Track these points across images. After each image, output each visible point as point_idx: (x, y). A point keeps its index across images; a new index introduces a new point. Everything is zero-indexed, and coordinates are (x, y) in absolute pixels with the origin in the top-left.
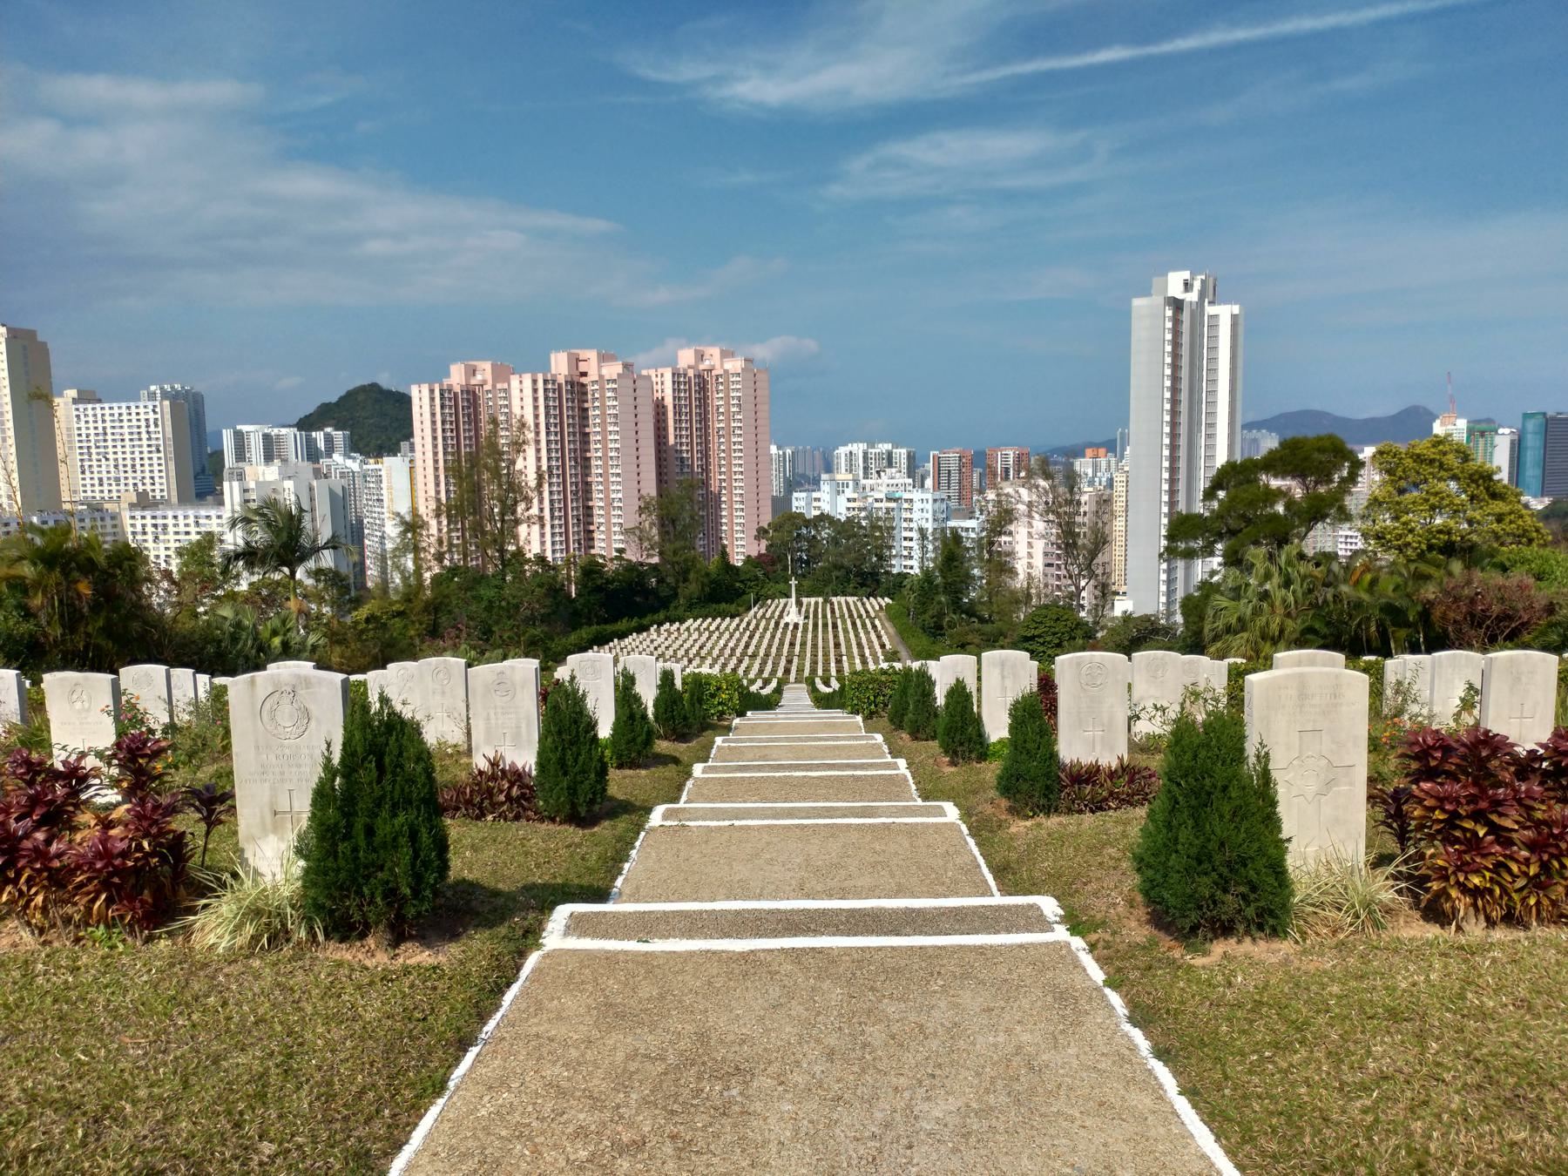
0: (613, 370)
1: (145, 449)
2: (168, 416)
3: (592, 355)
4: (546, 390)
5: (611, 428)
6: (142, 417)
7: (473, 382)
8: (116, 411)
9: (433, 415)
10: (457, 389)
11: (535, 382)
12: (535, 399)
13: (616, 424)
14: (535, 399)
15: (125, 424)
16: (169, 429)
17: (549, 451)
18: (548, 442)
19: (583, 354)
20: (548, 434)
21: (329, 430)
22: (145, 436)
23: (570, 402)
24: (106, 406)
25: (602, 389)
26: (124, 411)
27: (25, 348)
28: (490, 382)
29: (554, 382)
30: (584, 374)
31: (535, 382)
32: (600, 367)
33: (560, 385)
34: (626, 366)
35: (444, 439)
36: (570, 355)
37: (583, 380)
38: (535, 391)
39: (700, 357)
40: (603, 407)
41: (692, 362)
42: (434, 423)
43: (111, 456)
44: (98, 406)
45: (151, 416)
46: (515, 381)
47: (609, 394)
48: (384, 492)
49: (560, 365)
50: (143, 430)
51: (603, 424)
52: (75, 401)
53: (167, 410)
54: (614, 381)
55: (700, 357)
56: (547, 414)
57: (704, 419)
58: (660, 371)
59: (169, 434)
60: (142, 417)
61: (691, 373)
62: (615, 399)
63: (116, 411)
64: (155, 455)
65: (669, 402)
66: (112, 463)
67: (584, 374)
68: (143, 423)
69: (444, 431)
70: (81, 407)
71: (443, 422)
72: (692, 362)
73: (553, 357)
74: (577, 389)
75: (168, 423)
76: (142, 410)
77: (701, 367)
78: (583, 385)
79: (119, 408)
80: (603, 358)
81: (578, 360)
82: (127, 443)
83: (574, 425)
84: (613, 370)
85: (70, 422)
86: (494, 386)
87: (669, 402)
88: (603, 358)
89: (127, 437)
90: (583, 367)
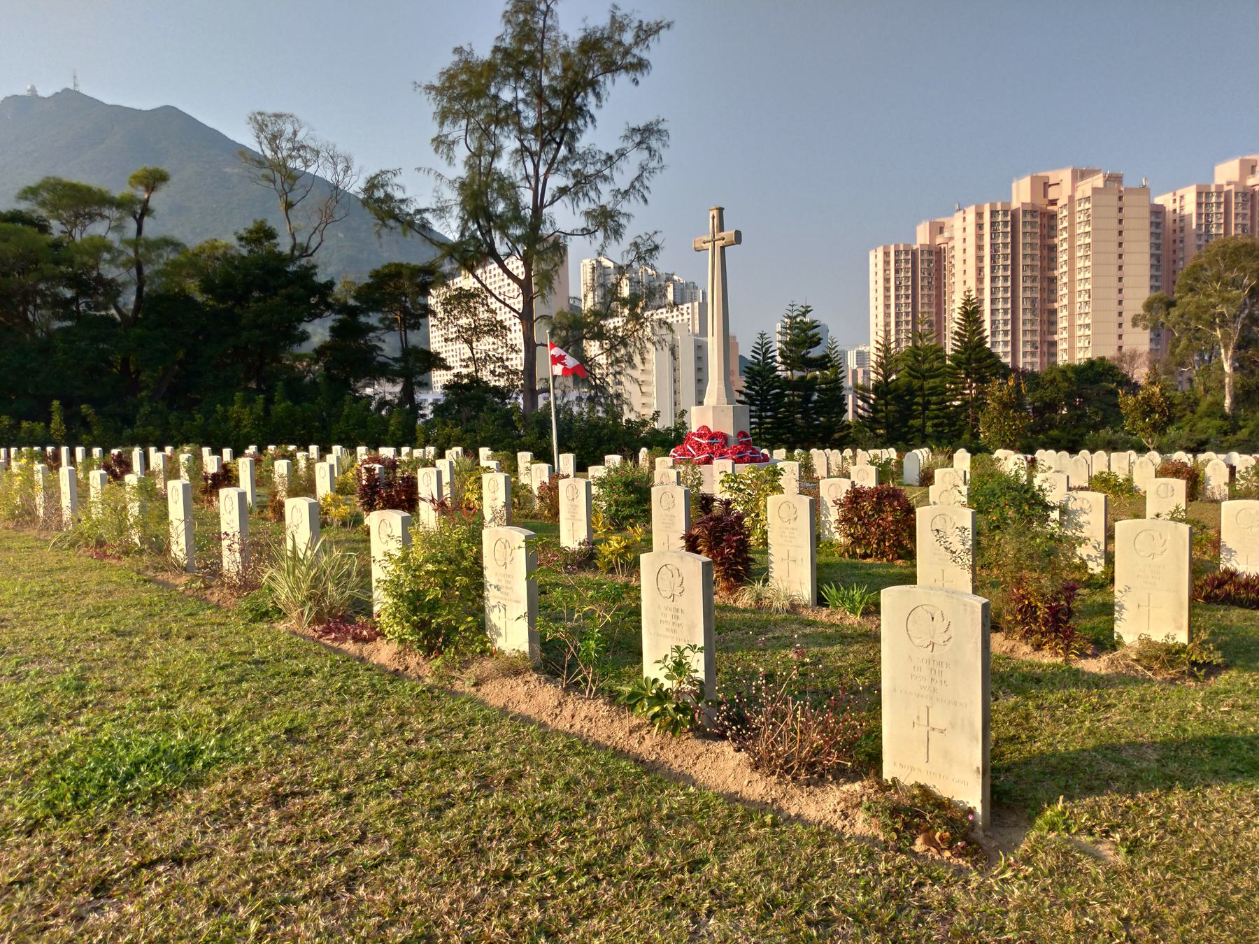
2: (697, 316)
3: (1065, 175)
9: (887, 280)
19: (1053, 177)
30: (1053, 202)
32: (1074, 189)
36: (1034, 180)
41: (1236, 177)
42: (887, 289)
51: (1072, 258)
54: (1088, 199)
58: (1179, 193)
71: (897, 288)
72: (1235, 176)
73: (1014, 185)
74: (1043, 220)
80: (1080, 175)
81: (1047, 185)
83: (1033, 267)
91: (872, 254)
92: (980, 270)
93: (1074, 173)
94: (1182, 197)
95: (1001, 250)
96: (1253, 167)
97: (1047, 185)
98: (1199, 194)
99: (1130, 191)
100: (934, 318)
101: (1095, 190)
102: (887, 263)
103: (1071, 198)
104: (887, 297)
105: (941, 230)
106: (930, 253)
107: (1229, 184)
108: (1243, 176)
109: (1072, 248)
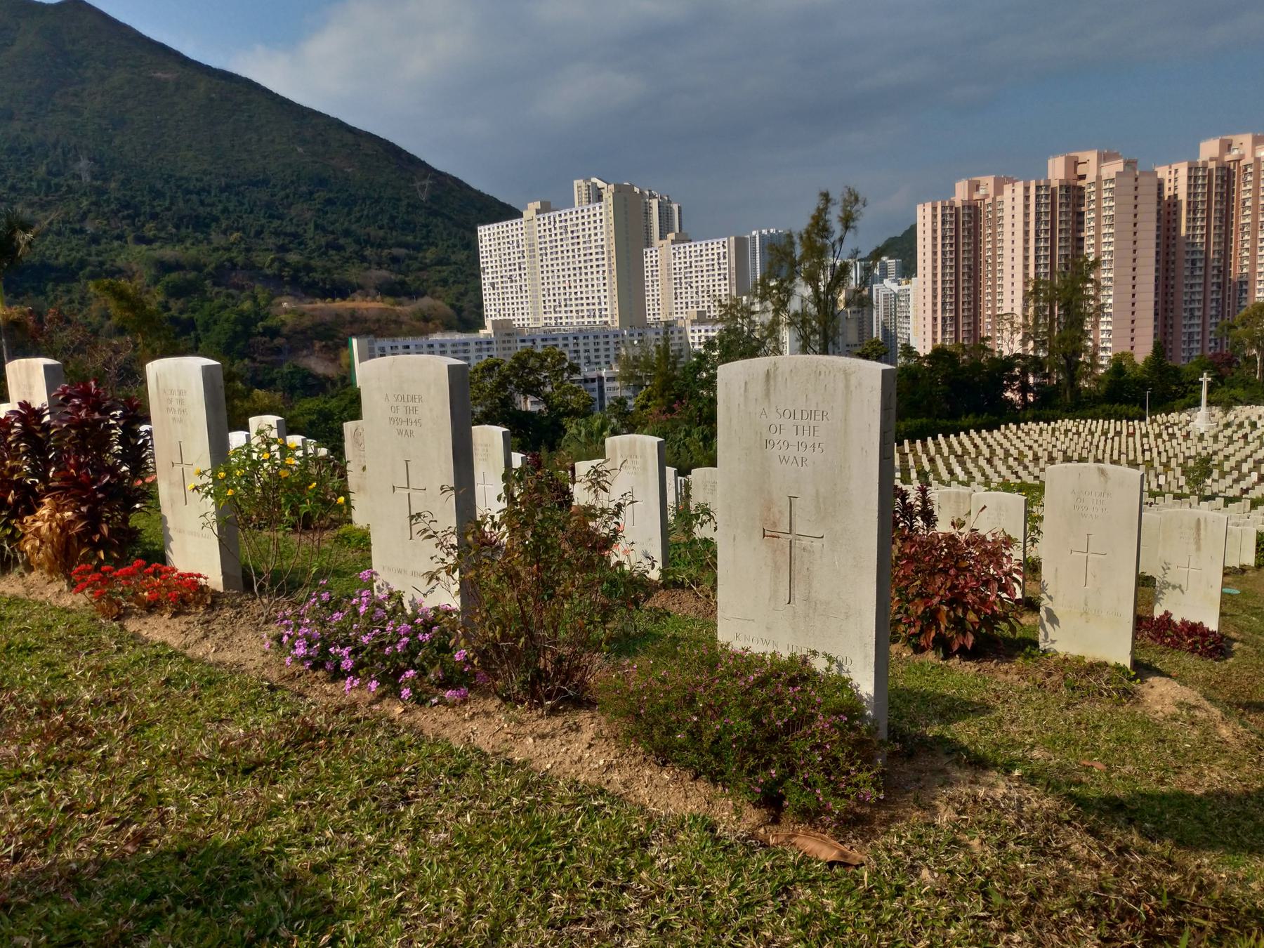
0: (1113, 168)
1: (717, 278)
2: (733, 250)
3: (1092, 156)
4: (1037, 196)
5: (1105, 231)
6: (715, 251)
7: (976, 197)
8: (699, 248)
9: (935, 231)
10: (959, 204)
11: (1027, 189)
12: (1027, 207)
13: (1111, 226)
14: (1027, 207)
15: (704, 258)
16: (733, 261)
17: (1037, 258)
18: (1037, 249)
19: (1082, 156)
20: (1037, 240)
21: (884, 259)
22: (716, 267)
23: (1065, 209)
24: (692, 244)
25: (1099, 190)
26: (704, 247)
27: (625, 199)
28: (992, 195)
29: (1047, 187)
30: (1083, 177)
31: (1027, 189)
32: (1099, 168)
33: (1054, 190)
34: (1127, 164)
35: (944, 253)
36: (1067, 159)
37: (1080, 183)
38: (1027, 198)
39: (1227, 147)
40: (1099, 207)
41: (1216, 153)
42: (935, 238)
43: (694, 285)
44: (687, 245)
45: (722, 250)
46: (1007, 189)
47: (1106, 195)
48: (911, 309)
49: (1056, 171)
50: (716, 262)
51: (1098, 228)
52: (673, 242)
53: (733, 245)
54: (1112, 180)
55: (1227, 147)
56: (1038, 221)
57: (1226, 218)
58: (1174, 166)
59: (733, 265)
60: (715, 251)
61: (1212, 165)
62: (1112, 199)
63: (699, 248)
64: (722, 282)
65: (1183, 196)
66: (694, 290)
67: (1083, 177)
68: (716, 257)
69: (943, 245)
70: (676, 246)
71: (943, 238)
72: (1216, 153)
73: (1050, 162)
74: (1073, 194)
75: (733, 255)
76: (715, 246)
77: (1227, 158)
78: (1082, 189)
79: (699, 246)
80: (1104, 158)
81: (1077, 163)
82: (705, 273)
83: (1066, 231)
84: (1113, 168)
85: (668, 259)
86: (994, 199)
87: (1183, 196)
88: (1104, 158)
89: (705, 268)
90: (1081, 170)
91: (920, 209)
92: (1026, 233)
93: (1099, 155)
94: (1176, 171)
95: (1043, 218)
96: (1230, 146)
97: (1077, 163)
98: (1190, 169)
99: (1142, 173)
100: (972, 262)
101: (1118, 173)
102: (935, 216)
103: (1099, 177)
104: (935, 246)
105: (977, 188)
106: (969, 207)
107: (1212, 159)
108: (1222, 154)
109: (1099, 217)
